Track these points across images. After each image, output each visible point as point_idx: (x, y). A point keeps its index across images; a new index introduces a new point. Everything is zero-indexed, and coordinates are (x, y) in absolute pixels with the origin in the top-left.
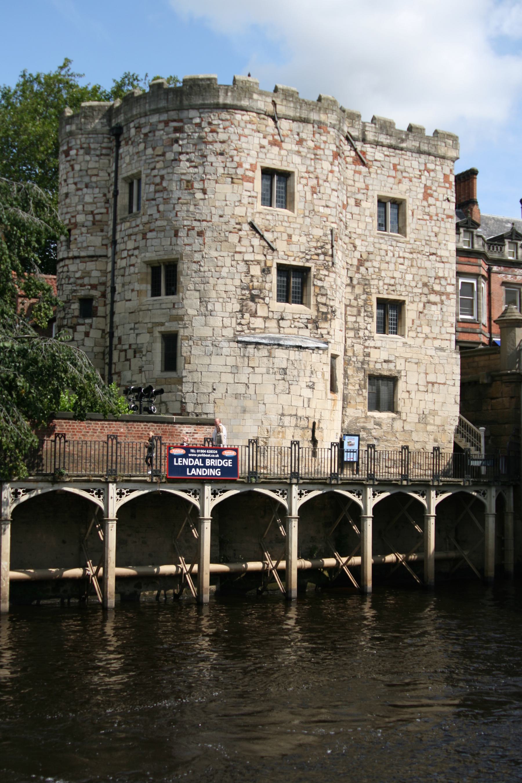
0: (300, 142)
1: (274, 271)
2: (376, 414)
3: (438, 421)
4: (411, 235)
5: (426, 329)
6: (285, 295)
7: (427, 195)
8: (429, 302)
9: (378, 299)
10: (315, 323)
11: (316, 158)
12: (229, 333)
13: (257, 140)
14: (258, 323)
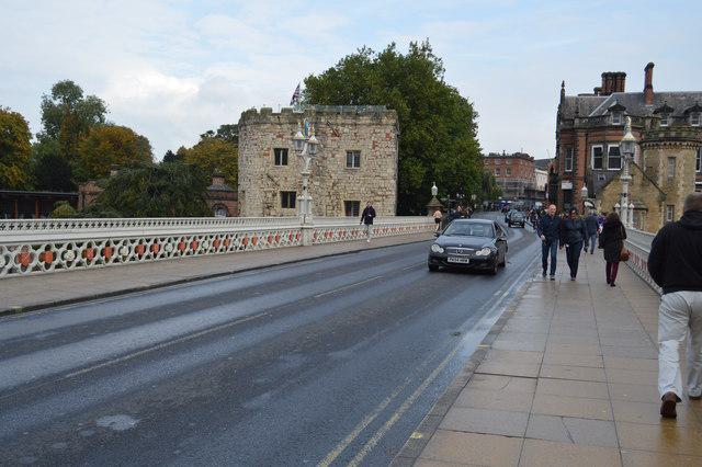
1: (278, 195)
6: (284, 205)
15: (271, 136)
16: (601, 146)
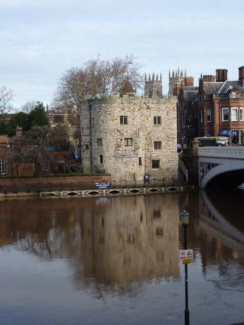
0: (129, 108)
1: (123, 140)
2: (154, 169)
3: (172, 170)
4: (163, 125)
5: (168, 148)
8: (169, 141)
9: (155, 142)
10: (134, 151)
12: (113, 155)
13: (118, 109)
14: (120, 152)
16: (228, 109)
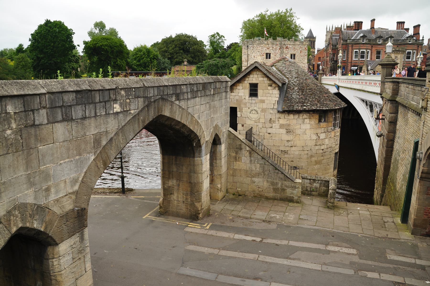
0: (273, 48)
7: (301, 52)
11: (276, 50)
15: (265, 48)
16: (358, 50)
